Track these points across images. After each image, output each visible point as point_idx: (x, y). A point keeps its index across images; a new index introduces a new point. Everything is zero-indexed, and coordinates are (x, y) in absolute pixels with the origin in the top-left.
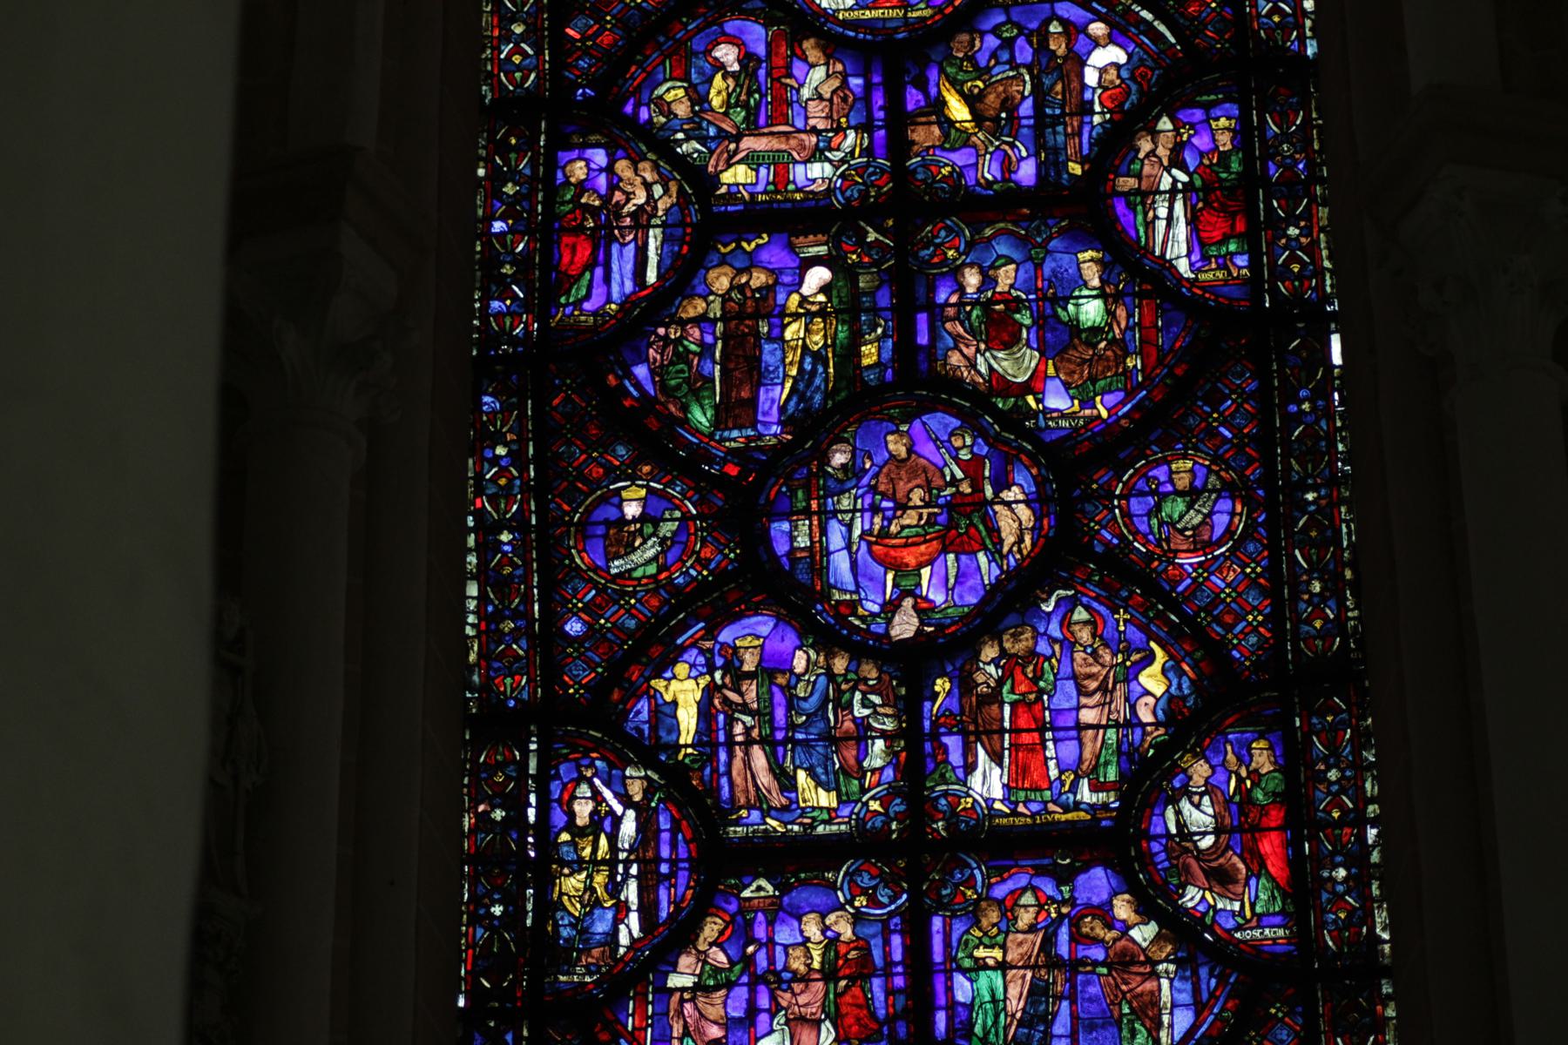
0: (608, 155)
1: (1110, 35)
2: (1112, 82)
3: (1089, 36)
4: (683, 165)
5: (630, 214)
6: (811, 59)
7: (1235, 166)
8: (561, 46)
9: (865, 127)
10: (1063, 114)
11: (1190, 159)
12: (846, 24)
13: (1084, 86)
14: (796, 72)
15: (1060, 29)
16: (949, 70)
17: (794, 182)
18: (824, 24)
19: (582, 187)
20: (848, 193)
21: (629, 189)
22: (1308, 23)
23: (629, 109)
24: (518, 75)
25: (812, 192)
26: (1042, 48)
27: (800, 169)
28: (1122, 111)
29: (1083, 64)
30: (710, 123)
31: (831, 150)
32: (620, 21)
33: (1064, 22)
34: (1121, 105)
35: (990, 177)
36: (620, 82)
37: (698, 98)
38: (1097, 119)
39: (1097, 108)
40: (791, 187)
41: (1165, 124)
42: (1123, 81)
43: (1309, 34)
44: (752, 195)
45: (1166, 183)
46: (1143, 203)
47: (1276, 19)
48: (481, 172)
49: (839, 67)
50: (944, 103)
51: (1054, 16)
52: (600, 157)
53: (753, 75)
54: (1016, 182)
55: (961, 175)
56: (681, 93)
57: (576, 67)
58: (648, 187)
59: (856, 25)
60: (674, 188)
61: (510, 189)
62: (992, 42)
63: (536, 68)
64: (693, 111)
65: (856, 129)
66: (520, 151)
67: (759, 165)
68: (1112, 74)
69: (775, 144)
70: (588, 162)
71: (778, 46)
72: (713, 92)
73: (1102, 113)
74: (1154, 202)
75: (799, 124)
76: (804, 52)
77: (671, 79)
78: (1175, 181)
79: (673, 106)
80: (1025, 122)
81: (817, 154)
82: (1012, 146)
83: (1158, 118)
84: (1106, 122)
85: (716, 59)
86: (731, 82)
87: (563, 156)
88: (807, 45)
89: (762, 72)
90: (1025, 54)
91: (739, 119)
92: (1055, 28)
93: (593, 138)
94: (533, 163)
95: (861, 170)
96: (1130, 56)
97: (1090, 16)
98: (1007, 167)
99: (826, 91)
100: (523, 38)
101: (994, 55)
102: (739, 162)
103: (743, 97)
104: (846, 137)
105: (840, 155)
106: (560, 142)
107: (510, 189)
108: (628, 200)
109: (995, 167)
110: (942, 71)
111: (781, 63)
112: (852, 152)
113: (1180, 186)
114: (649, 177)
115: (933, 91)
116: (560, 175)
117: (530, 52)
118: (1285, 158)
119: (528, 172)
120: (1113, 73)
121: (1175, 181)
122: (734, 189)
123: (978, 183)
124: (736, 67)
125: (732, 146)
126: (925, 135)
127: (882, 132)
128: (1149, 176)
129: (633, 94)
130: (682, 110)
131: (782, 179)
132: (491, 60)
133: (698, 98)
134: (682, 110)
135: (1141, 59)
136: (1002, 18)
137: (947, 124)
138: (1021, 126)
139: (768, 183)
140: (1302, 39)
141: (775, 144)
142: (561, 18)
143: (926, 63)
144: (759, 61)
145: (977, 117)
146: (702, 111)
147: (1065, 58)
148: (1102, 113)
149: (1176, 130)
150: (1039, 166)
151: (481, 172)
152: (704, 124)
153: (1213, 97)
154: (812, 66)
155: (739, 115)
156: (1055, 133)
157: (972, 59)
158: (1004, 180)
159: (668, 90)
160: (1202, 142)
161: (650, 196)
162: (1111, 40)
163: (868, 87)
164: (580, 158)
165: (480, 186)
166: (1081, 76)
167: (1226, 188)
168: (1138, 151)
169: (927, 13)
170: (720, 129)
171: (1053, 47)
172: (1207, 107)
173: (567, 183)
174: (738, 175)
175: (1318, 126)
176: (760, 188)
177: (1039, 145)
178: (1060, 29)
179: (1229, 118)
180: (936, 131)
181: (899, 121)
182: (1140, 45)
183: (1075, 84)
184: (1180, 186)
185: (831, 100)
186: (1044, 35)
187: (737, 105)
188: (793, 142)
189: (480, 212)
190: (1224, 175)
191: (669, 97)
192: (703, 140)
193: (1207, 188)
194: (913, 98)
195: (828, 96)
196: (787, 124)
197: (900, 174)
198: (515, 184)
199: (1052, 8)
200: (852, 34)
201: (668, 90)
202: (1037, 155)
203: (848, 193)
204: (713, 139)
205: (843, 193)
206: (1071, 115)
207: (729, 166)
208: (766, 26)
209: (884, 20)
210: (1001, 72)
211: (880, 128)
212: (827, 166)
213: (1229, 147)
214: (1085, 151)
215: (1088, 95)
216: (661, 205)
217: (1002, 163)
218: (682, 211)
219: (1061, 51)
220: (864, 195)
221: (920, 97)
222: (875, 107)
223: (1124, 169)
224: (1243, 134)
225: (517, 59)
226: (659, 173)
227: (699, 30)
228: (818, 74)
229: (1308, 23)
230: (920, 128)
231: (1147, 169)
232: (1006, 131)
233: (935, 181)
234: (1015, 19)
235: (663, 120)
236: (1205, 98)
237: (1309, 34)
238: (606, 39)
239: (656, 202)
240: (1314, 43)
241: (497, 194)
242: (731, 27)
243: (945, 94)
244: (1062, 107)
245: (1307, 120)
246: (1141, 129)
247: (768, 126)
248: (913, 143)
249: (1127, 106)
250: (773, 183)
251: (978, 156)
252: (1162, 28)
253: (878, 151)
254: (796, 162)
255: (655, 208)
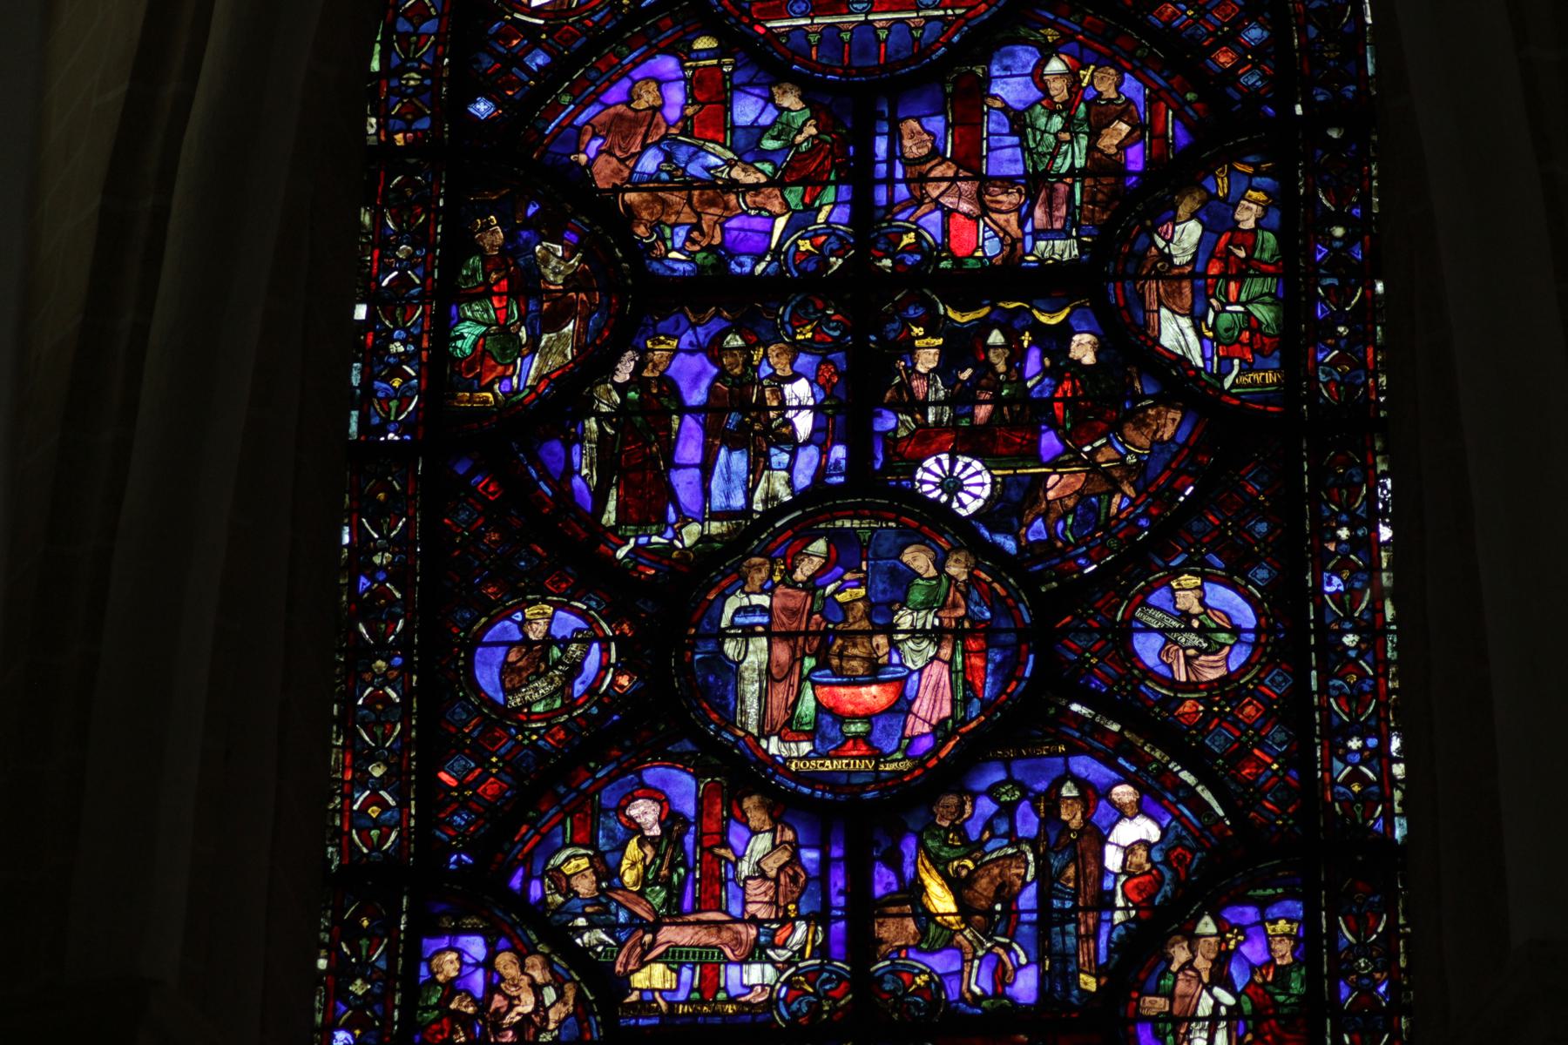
0: (487, 945)
1: (1139, 803)
2: (1140, 866)
3: (1112, 803)
4: (582, 959)
5: (513, 1027)
6: (753, 824)
7: (1296, 986)
8: (431, 794)
9: (818, 918)
10: (1075, 908)
11: (1239, 978)
12: (799, 777)
13: (1103, 871)
14: (733, 840)
15: (1075, 793)
16: (930, 843)
17: (725, 989)
18: (772, 777)
19: (453, 987)
20: (795, 1006)
21: (513, 991)
22: (1398, 795)
23: (516, 883)
24: (374, 833)
25: (748, 1003)
26: (1050, 816)
27: (733, 971)
28: (1152, 907)
29: (1103, 840)
30: (619, 905)
31: (774, 947)
32: (508, 763)
33: (1080, 783)
34: (1152, 897)
35: (977, 990)
36: (507, 846)
37: (606, 871)
38: (1119, 917)
39: (1120, 902)
40: (721, 996)
41: (1207, 926)
42: (1154, 865)
43: (1398, 809)
44: (671, 1004)
45: (1205, 1007)
46: (1175, 1033)
47: (1356, 788)
48: (322, 964)
49: (789, 835)
50: (923, 888)
51: (1068, 775)
52: (476, 947)
53: (680, 841)
54: (1012, 999)
55: (941, 986)
56: (584, 863)
57: (450, 824)
58: (537, 989)
59: (811, 778)
60: (570, 994)
61: (358, 987)
62: (987, 806)
63: (399, 823)
64: (598, 888)
65: (807, 919)
66: (373, 936)
67: (682, 965)
68: (1140, 856)
69: (704, 936)
70: (461, 953)
71: (711, 805)
72: (625, 863)
73: (1126, 909)
74: (1189, 1031)
75: (735, 910)
76: (744, 813)
77: (572, 845)
78: (1217, 1003)
79: (574, 881)
80: (1025, 917)
81: (755, 953)
82: (1008, 949)
83: (1197, 918)
84: (1129, 920)
85: (631, 819)
86: (648, 850)
87: (430, 945)
88: (748, 803)
89: (689, 840)
90: (1028, 825)
91: (658, 901)
92: (1069, 790)
93: (469, 922)
94: (390, 954)
95: (812, 975)
96: (1164, 832)
97: (1114, 775)
98: (1002, 978)
99: (771, 867)
100: (383, 782)
101: (989, 825)
102: (655, 960)
103: (664, 872)
104: (794, 930)
105: (786, 954)
106: (426, 926)
107: (358, 987)
108: (511, 1007)
109: (985, 973)
110: (921, 844)
111: (715, 827)
112: (802, 951)
113: (1223, 1010)
114: (539, 976)
115: (909, 871)
116: (424, 971)
117: (393, 803)
118: (1361, 977)
119: (382, 964)
120: (1141, 854)
121: (1217, 1003)
122: (648, 996)
123: (962, 998)
124: (656, 831)
125: (648, 938)
126: (895, 931)
127: (842, 924)
128: (1183, 996)
129: (522, 863)
130: (585, 886)
131: (710, 984)
132: (341, 811)
133: (606, 871)
134: (585, 886)
135: (1179, 837)
136: (1000, 776)
137: (925, 917)
138: (1020, 923)
139: (692, 990)
140: (1389, 816)
141: (704, 936)
142: (432, 761)
143: (899, 834)
144: (686, 823)
145: (965, 909)
146: (611, 888)
147: (1080, 832)
148: (1126, 909)
149: (1221, 933)
150: (1041, 978)
151: (322, 964)
152: (613, 907)
153: (1270, 891)
154: (754, 833)
155: (658, 896)
156: (1064, 933)
157: (960, 830)
158: (998, 995)
159: (568, 859)
160: (1254, 952)
161: (539, 1002)
162: (1142, 809)
163: (825, 862)
164: (451, 949)
165: (320, 982)
166: (1101, 857)
167: (1284, 1017)
168: (1170, 961)
169: (905, 765)
170: (633, 915)
171: (1064, 817)
172: (1263, 904)
173: (433, 981)
174: (654, 977)
175: (1405, 935)
176: (681, 995)
177: (1042, 950)
178: (1075, 793)
179: (1290, 921)
180: (911, 925)
181: (864, 910)
182: (1179, 817)
183: (1091, 868)
184: (1223, 1010)
185: (776, 880)
186: (1054, 800)
187: (655, 882)
188: (726, 935)
189: (319, 1018)
190: (1281, 998)
191: (569, 869)
192: (611, 929)
193: (1258, 1014)
194: (883, 881)
195: (773, 874)
196: (719, 910)
197: (862, 981)
198: (366, 981)
199: (1066, 764)
200: (806, 791)
201: (568, 859)
202: (1039, 962)
203: (795, 1006)
204: (623, 927)
205: (788, 1007)
206: (1086, 910)
207: (643, 964)
208: (697, 777)
209: (849, 773)
210: (997, 848)
211: (838, 919)
212: (769, 968)
213: (1288, 960)
214: (1103, 960)
215: (1108, 883)
216: (553, 1015)
217: (994, 972)
218: (580, 1023)
219: (1076, 823)
220: (815, 1009)
221: (892, 879)
222: (834, 891)
223: (1151, 984)
224: (1308, 944)
225: (374, 811)
226: (552, 972)
227: (610, 778)
228: (762, 843)
229: (1398, 795)
230: (890, 921)
231: (1181, 987)
232: (1001, 928)
233: (906, 994)
234: (1017, 777)
235: (559, 899)
236: (1260, 892)
237: (1398, 809)
238: (490, 788)
239: (547, 1010)
240: (1404, 822)
241: (342, 994)
242: (651, 775)
243: (924, 875)
244: (1075, 898)
245: (1392, 926)
246: (1176, 932)
247: (694, 911)
248: (881, 941)
249: (1158, 900)
250: (698, 990)
251: (963, 961)
252: (1207, 795)
253: (837, 949)
254: (728, 962)
255: (546, 1019)
